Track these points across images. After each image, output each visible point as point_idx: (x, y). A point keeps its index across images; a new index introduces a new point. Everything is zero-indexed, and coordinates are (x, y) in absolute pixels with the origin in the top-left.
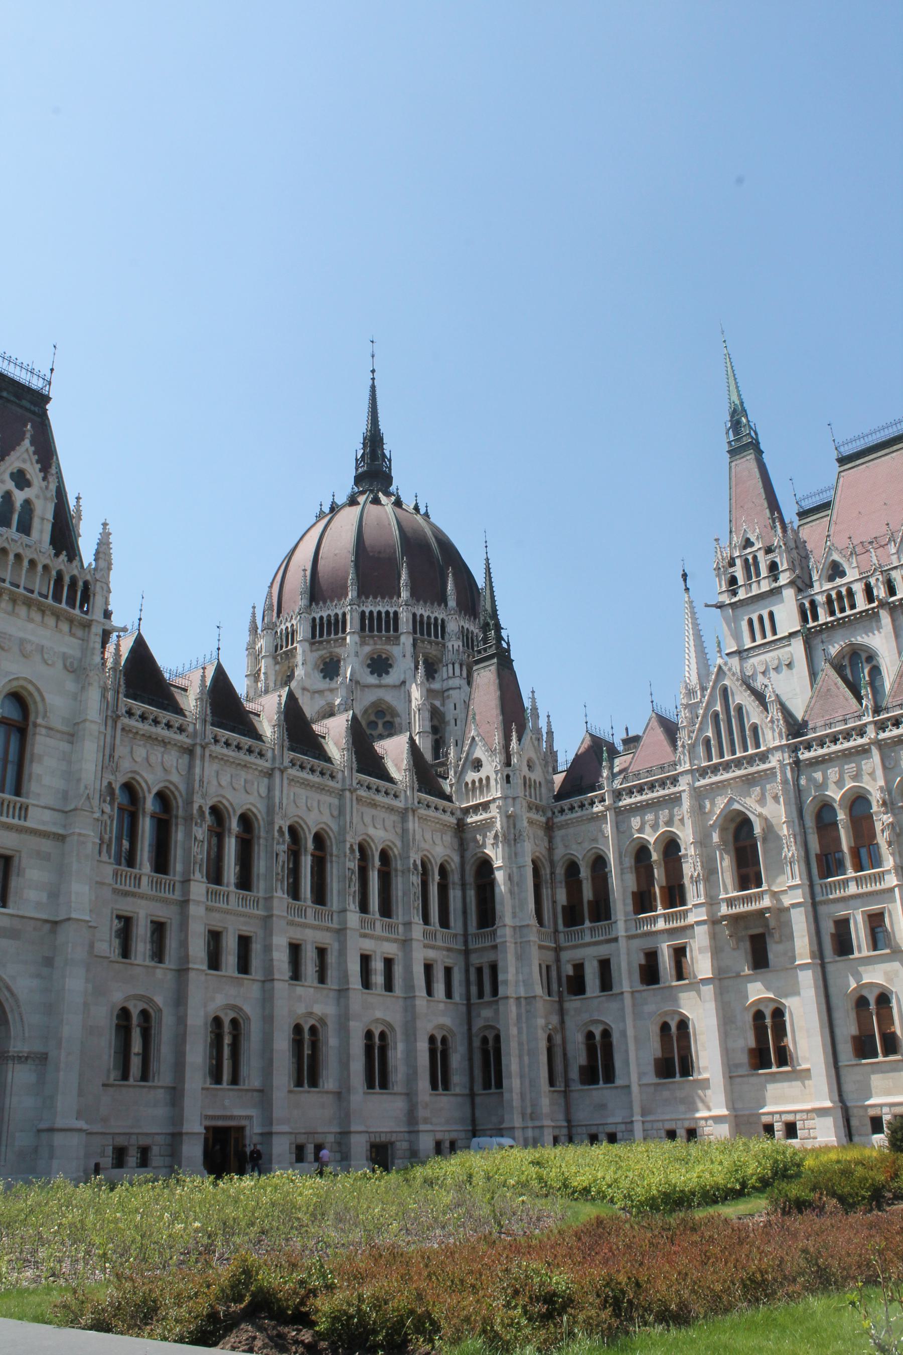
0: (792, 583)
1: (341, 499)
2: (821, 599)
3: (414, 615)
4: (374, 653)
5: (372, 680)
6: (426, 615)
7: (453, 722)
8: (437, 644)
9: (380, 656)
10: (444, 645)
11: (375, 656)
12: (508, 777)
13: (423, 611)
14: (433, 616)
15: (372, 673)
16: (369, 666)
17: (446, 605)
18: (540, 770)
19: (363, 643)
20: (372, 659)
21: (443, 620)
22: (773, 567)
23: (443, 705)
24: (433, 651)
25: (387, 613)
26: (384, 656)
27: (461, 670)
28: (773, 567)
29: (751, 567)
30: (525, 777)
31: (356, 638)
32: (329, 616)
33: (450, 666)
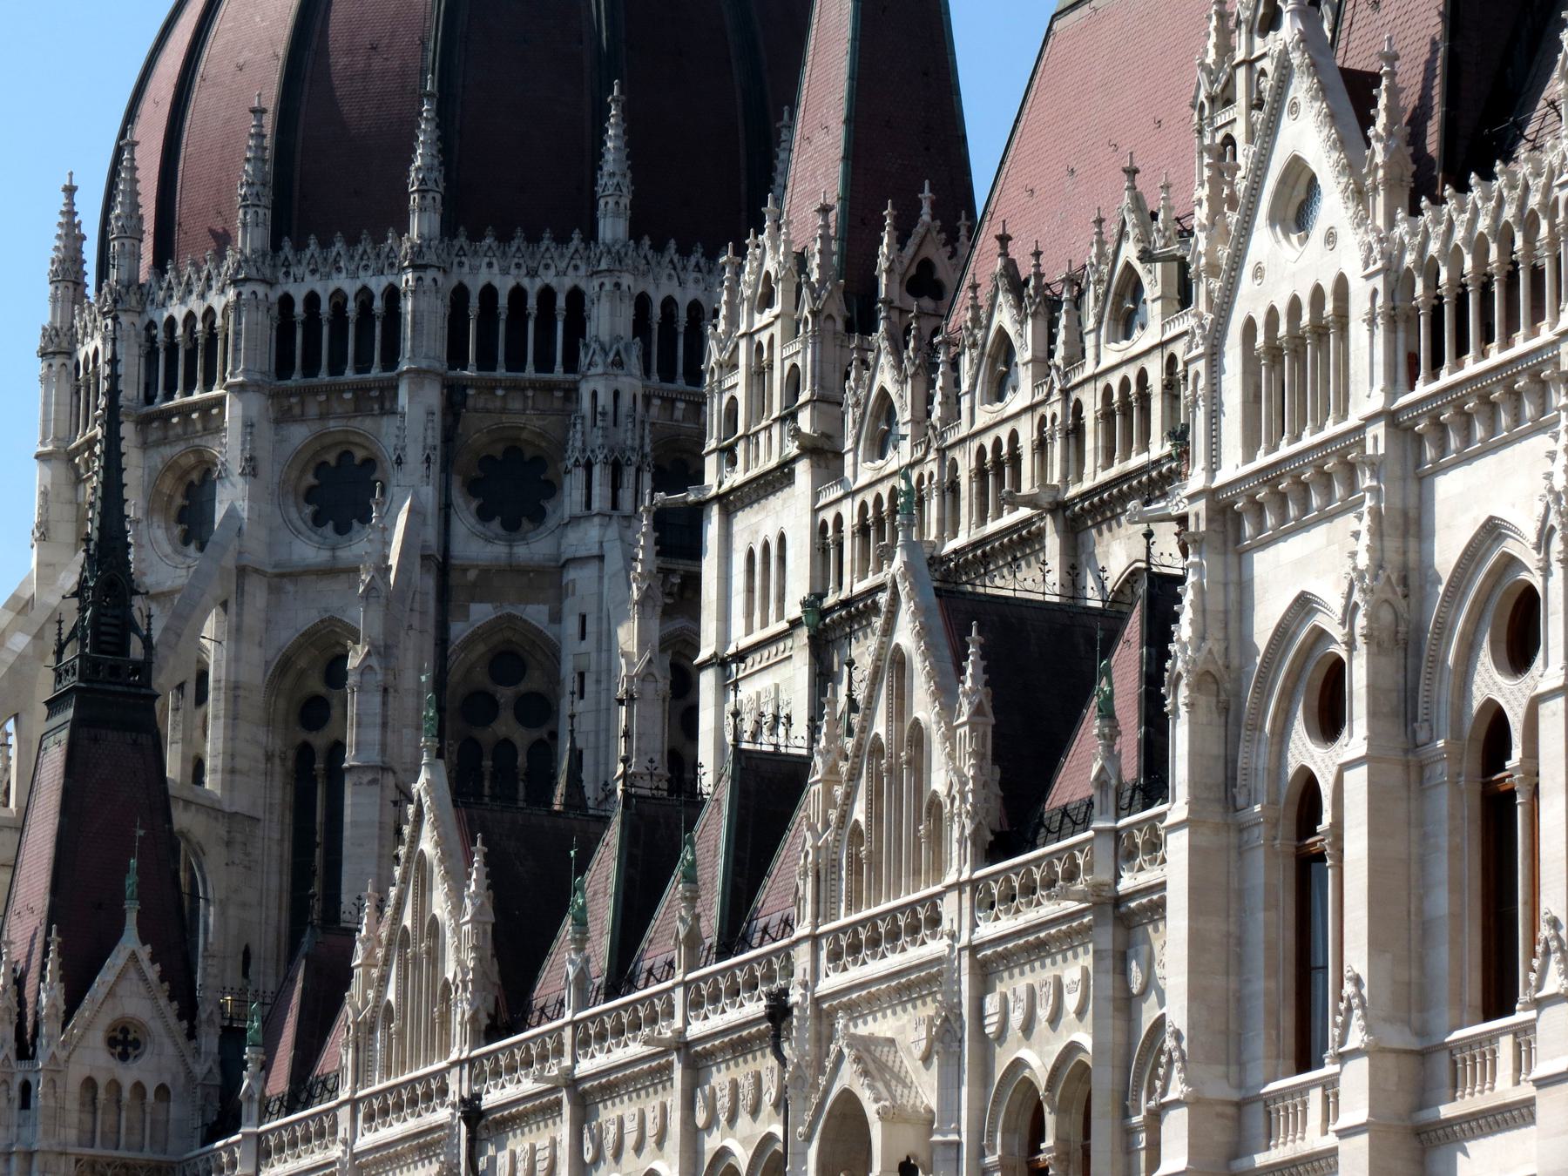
3: (460, 293)
4: (326, 449)
5: (308, 551)
6: (504, 285)
8: (549, 387)
9: (346, 455)
10: (571, 392)
11: (331, 458)
13: (492, 272)
14: (532, 288)
15: (318, 521)
16: (310, 496)
17: (591, 235)
18: (169, 1049)
19: (283, 418)
20: (321, 468)
21: (576, 296)
23: (556, 617)
25: (365, 295)
26: (360, 454)
27: (616, 486)
30: (90, 1084)
31: (257, 402)
32: (190, 316)
33: (580, 473)
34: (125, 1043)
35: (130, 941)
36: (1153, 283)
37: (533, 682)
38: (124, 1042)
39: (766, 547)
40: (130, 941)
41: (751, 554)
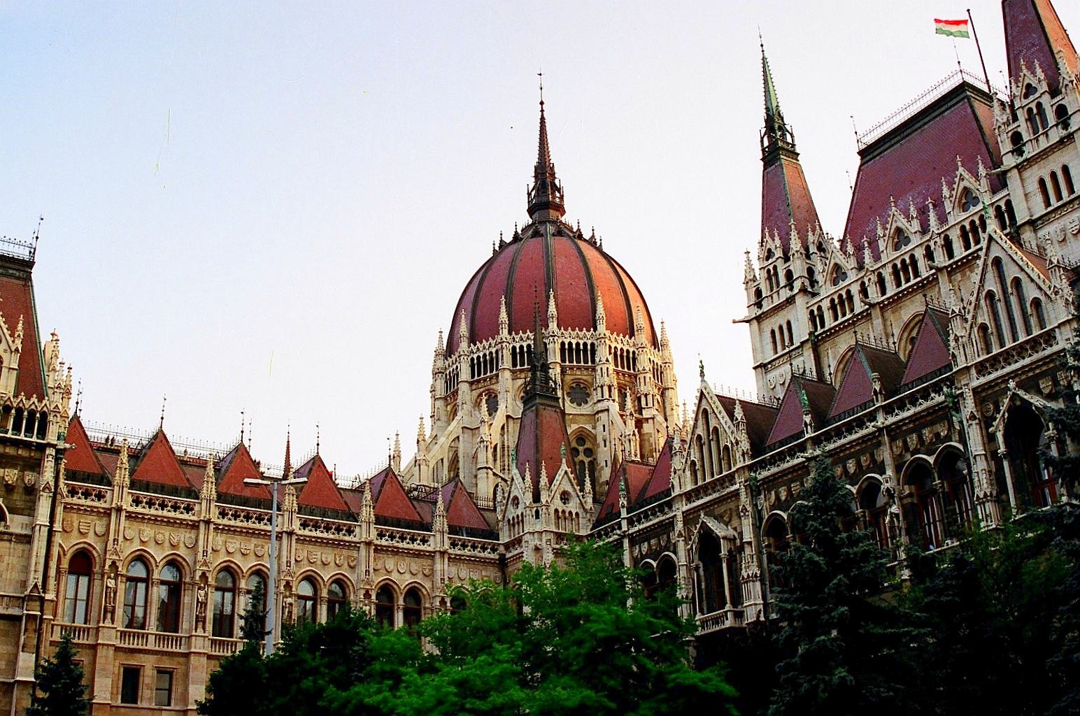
0: (803, 290)
1: (508, 238)
2: (826, 304)
7: (602, 444)
8: (587, 369)
12: (537, 512)
22: (789, 275)
24: (584, 376)
28: (789, 275)
29: (772, 276)
30: (556, 511)
33: (599, 389)
34: (565, 499)
35: (564, 467)
36: (982, 187)
37: (588, 445)
38: (565, 497)
39: (781, 328)
40: (564, 467)
41: (773, 332)
